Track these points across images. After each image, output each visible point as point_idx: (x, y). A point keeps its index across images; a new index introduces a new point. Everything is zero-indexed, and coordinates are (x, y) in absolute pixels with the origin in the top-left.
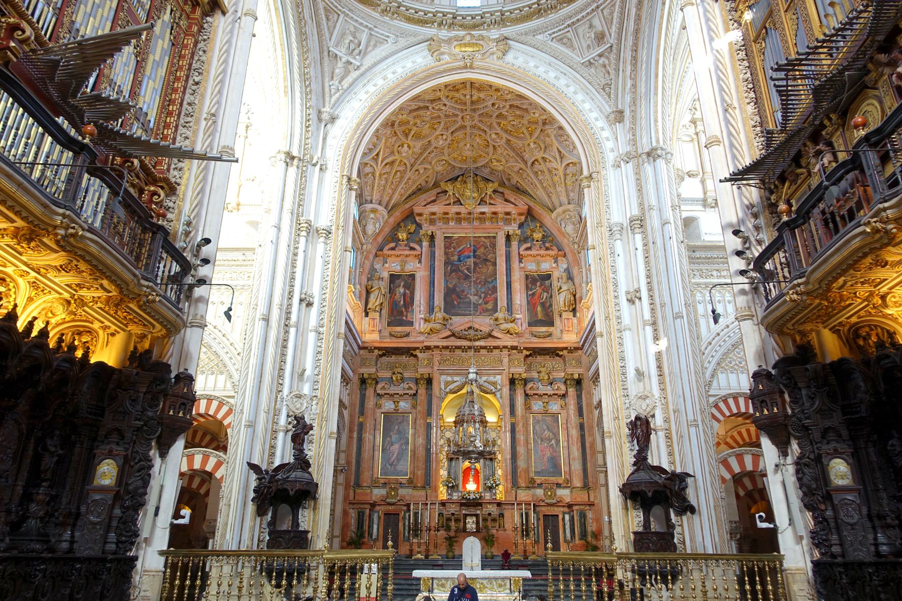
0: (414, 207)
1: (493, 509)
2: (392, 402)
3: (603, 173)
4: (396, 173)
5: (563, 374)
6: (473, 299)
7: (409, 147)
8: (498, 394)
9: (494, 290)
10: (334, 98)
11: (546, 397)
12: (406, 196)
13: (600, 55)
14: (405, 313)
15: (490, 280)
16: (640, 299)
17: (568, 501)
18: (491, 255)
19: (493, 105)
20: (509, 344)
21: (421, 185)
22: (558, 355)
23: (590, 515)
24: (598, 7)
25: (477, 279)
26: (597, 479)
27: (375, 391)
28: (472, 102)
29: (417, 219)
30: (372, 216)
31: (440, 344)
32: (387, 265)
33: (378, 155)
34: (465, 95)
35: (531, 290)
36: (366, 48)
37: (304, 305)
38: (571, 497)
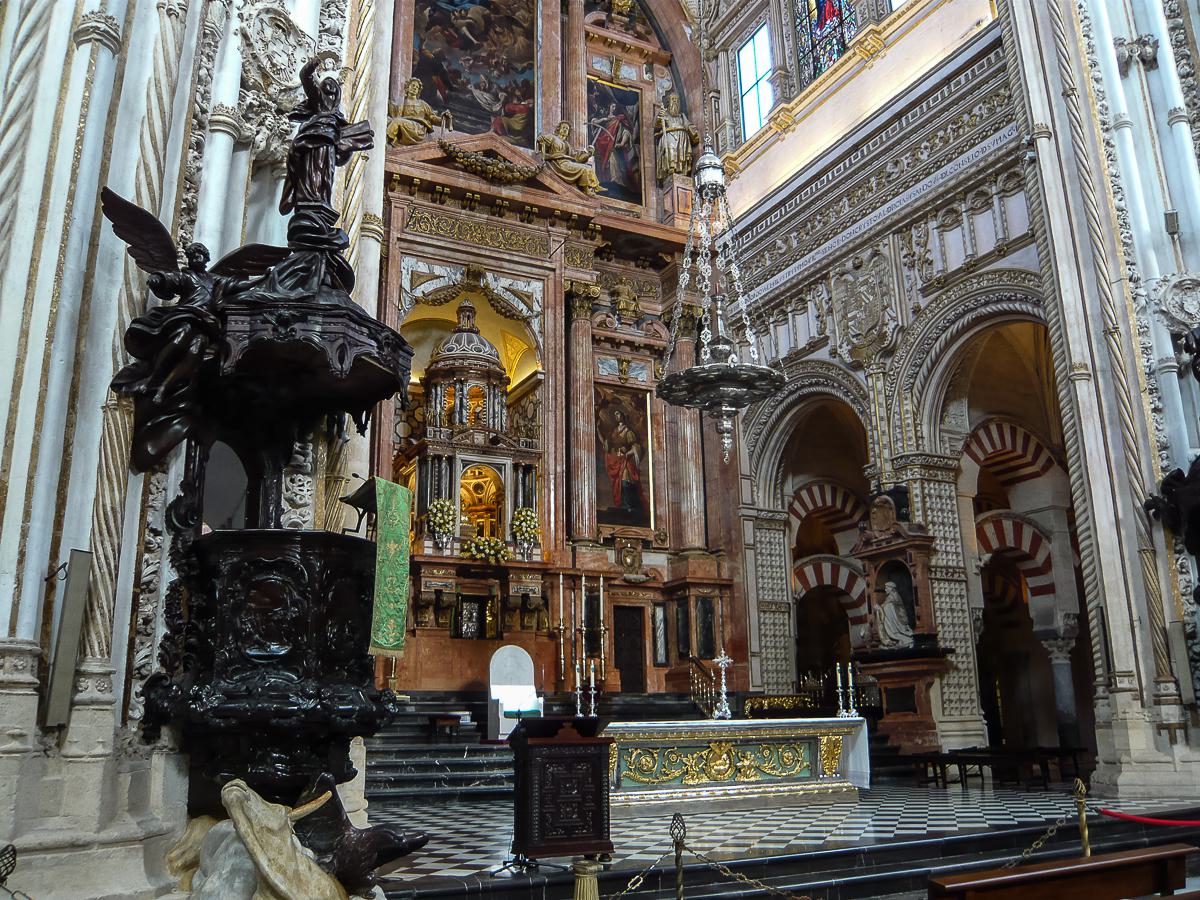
1: (533, 585)
5: (660, 308)
6: (482, 97)
8: (535, 325)
9: (528, 91)
11: (628, 349)
15: (519, 66)
16: (1151, 63)
17: (666, 580)
18: (523, 12)
20: (576, 208)
22: (658, 265)
23: (719, 608)
25: (491, 55)
26: (740, 532)
31: (416, 173)
35: (598, 116)
38: (673, 571)
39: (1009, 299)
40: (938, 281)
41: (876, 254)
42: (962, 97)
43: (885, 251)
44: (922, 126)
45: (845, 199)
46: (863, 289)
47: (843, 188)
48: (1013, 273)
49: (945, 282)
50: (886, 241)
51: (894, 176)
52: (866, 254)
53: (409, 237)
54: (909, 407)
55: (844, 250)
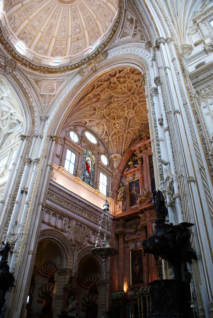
0: (131, 149)
2: (133, 244)
3: (147, 72)
4: (119, 138)
7: (118, 123)
10: (46, 110)
12: (129, 145)
14: (137, 198)
19: (137, 86)
21: (134, 138)
27: (124, 240)
28: (130, 91)
29: (135, 153)
30: (115, 159)
32: (127, 179)
33: (106, 132)
34: (122, 89)
36: (57, 87)
37: (24, 194)
53: (151, 219)
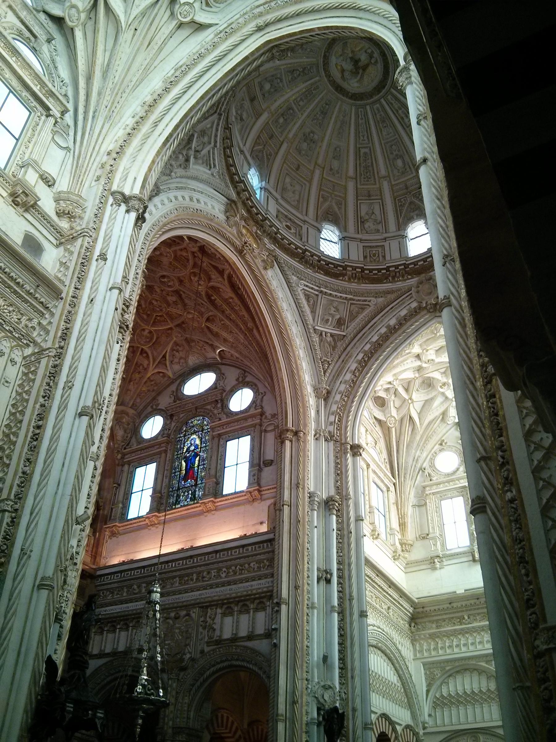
13: (332, 335)
16: (328, 581)
24: (351, 299)
39: (248, 662)
40: (216, 641)
41: (188, 615)
42: (248, 556)
43: (193, 615)
44: (226, 561)
45: (177, 579)
46: (177, 631)
47: (178, 573)
48: (253, 651)
49: (219, 642)
50: (195, 610)
51: (206, 579)
52: (183, 613)
54: (187, 701)
55: (171, 606)
